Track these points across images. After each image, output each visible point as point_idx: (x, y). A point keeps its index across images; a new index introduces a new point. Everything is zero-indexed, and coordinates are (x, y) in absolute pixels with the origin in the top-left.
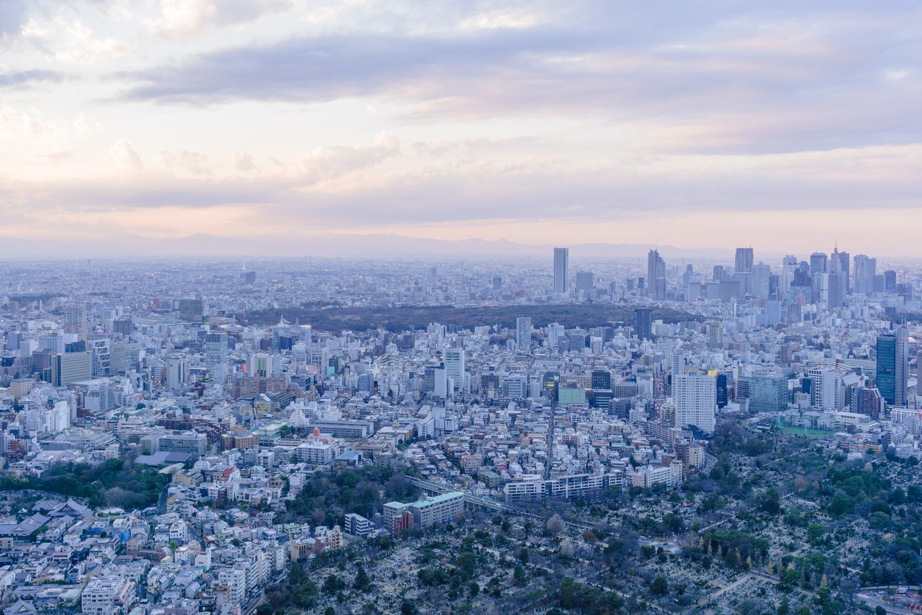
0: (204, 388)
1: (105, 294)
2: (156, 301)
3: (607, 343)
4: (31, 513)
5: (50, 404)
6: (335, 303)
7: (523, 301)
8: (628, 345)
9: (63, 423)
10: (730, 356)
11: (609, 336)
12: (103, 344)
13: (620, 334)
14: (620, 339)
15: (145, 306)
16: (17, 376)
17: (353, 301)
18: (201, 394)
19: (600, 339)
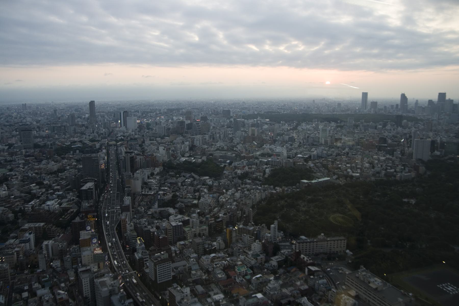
0: (233, 139)
1: (197, 109)
2: (214, 111)
3: (384, 128)
4: (180, 177)
5: (183, 143)
6: (278, 112)
7: (349, 112)
8: (392, 129)
9: (187, 149)
10: (436, 134)
11: (385, 125)
12: (198, 124)
13: (389, 125)
14: (389, 127)
15: (210, 112)
16: (172, 134)
17: (284, 111)
18: (232, 142)
19: (381, 126)
